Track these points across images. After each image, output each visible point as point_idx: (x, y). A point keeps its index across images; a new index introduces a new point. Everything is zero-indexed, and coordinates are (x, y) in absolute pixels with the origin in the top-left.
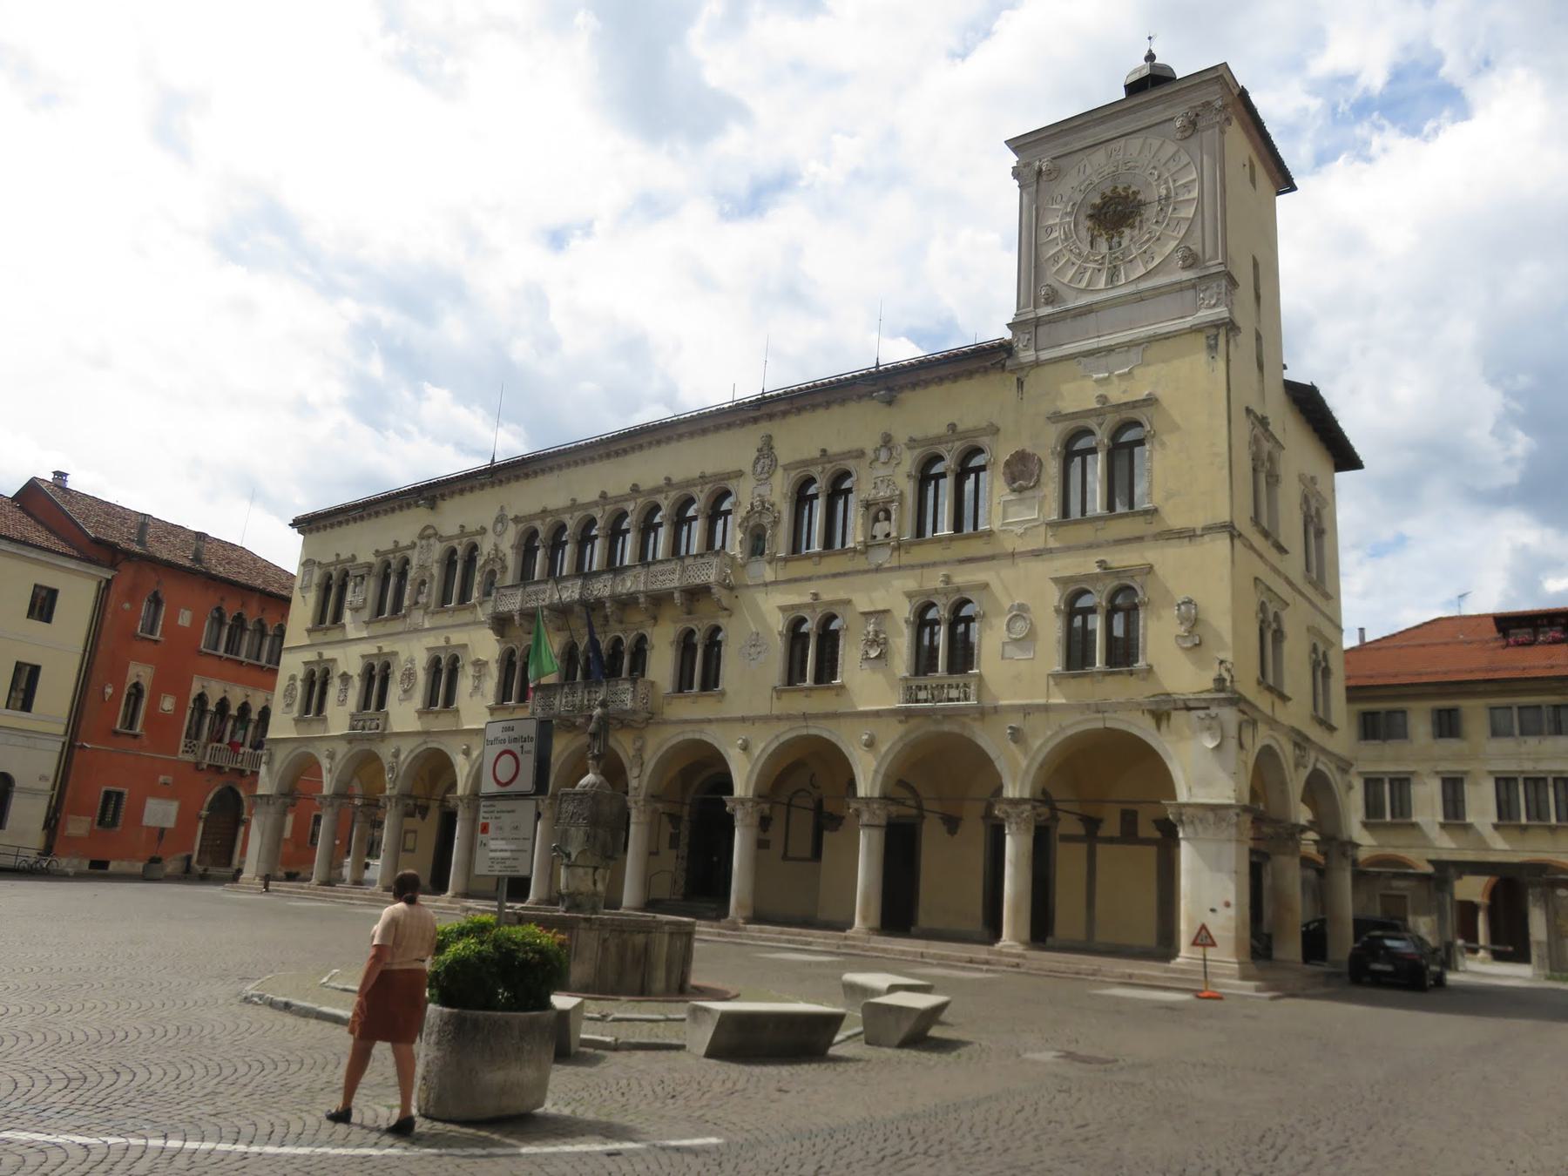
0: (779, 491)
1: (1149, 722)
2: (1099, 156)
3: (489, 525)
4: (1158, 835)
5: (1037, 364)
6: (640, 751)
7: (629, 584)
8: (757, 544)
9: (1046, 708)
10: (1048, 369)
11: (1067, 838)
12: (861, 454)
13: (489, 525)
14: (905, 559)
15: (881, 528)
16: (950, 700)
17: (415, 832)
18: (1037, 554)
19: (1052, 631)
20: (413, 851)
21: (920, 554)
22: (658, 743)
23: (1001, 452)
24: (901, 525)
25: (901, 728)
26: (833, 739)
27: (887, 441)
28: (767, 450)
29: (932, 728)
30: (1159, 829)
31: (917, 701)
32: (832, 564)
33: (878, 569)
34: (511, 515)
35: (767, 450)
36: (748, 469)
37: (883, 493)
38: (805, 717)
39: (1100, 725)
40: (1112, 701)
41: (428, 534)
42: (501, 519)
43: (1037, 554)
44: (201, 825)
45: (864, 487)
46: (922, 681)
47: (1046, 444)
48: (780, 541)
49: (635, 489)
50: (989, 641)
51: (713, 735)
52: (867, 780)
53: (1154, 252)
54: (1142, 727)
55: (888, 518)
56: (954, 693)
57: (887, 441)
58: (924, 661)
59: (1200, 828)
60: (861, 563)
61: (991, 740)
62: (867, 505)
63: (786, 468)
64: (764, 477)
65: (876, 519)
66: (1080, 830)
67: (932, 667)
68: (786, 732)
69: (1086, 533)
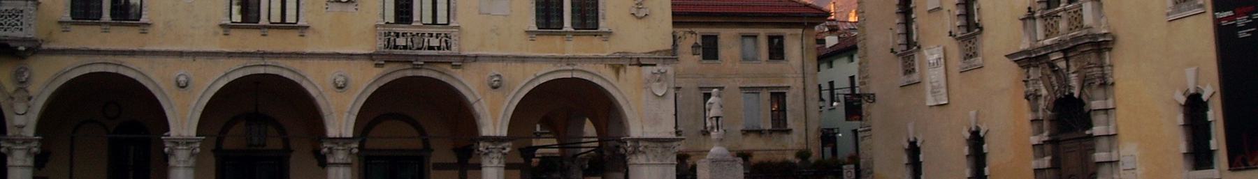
1: (608, 73)
4: (522, 161)
9: (523, 59)
11: (439, 167)
16: (431, 48)
25: (378, 72)
26: (296, 79)
29: (409, 73)
30: (522, 156)
31: (396, 47)
38: (263, 55)
39: (568, 75)
40: (570, 55)
46: (401, 29)
51: (135, 69)
52: (340, 121)
54: (603, 77)
56: (435, 42)
59: (651, 157)
61: (469, 83)
66: (453, 159)
68: (236, 70)
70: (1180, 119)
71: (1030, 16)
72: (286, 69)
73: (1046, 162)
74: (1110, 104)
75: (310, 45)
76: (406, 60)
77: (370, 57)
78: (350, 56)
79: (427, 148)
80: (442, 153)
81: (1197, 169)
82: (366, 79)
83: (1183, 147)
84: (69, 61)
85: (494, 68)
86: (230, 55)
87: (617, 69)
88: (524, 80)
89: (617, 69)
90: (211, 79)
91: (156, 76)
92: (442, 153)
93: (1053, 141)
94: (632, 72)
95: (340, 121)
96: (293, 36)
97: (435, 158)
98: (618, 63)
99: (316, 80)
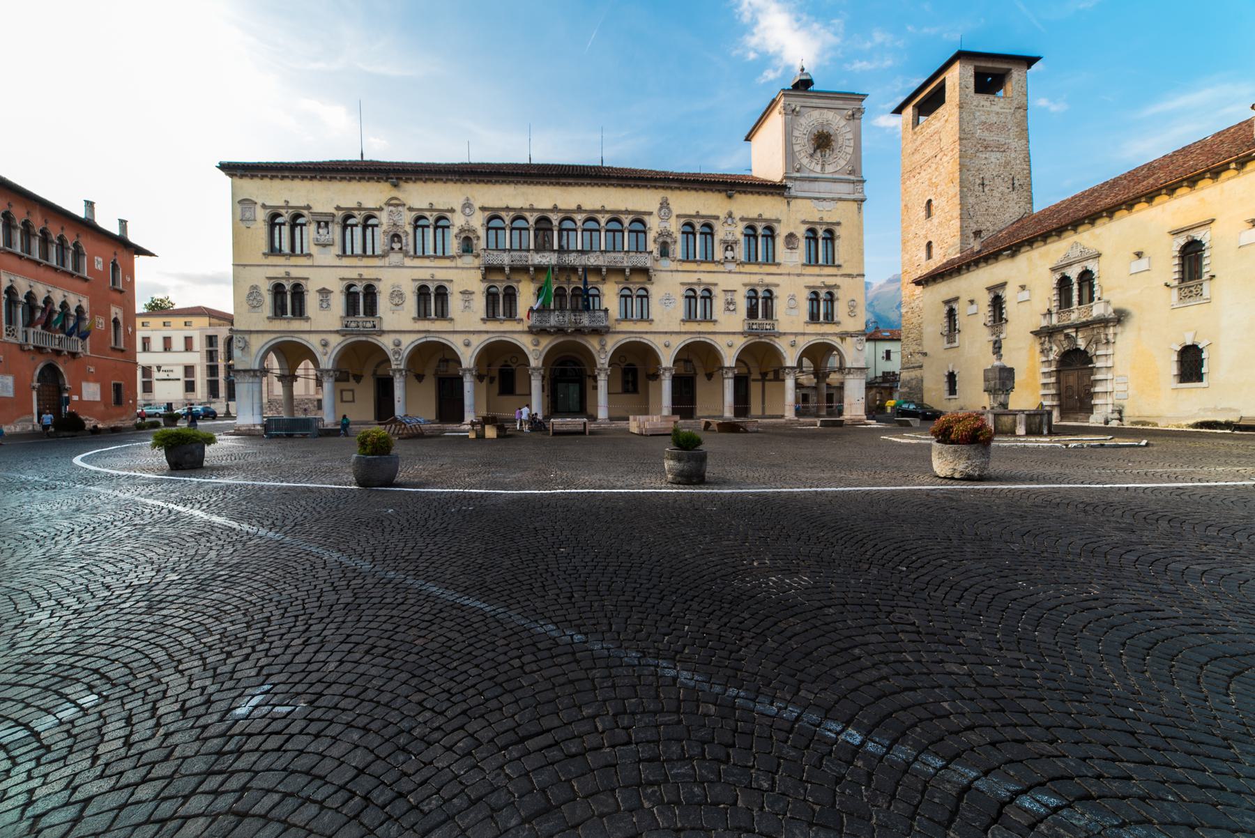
0: (674, 226)
1: (838, 340)
2: (816, 113)
3: (458, 207)
5: (796, 198)
6: (603, 346)
7: (592, 260)
8: (664, 252)
9: (804, 334)
10: (799, 201)
12: (717, 218)
13: (458, 207)
14: (742, 269)
15: (729, 254)
17: (352, 391)
18: (799, 275)
19: (805, 306)
20: (342, 401)
21: (748, 268)
22: (612, 343)
23: (781, 232)
24: (740, 252)
27: (730, 215)
28: (664, 205)
32: (704, 267)
33: (730, 272)
34: (477, 205)
35: (664, 205)
36: (655, 212)
37: (730, 238)
38: (699, 333)
41: (393, 203)
42: (467, 205)
43: (799, 275)
44: (35, 394)
45: (721, 232)
47: (801, 231)
48: (678, 250)
49: (579, 208)
50: (780, 307)
51: (647, 339)
52: (729, 359)
53: (837, 163)
54: (835, 341)
55: (732, 250)
57: (730, 215)
58: (752, 313)
60: (720, 268)
61: (782, 344)
62: (725, 242)
63: (678, 216)
64: (665, 218)
65: (726, 249)
67: (756, 317)
68: (688, 339)
69: (816, 270)
70: (1175, 357)
71: (1050, 312)
72: (708, 339)
73: (1053, 380)
74: (1110, 351)
75: (717, 328)
76: (757, 335)
77: (742, 333)
78: (734, 333)
79: (750, 372)
80: (755, 375)
81: (1181, 382)
82: (740, 342)
83: (1175, 372)
84: (622, 336)
85: (792, 338)
86: (686, 333)
87: (842, 339)
88: (803, 343)
89: (842, 339)
90: (678, 343)
91: (656, 342)
92: (755, 375)
93: (1058, 371)
94: (849, 339)
95: (729, 359)
96: (711, 325)
97: (753, 377)
98: (843, 336)
99: (720, 343)
